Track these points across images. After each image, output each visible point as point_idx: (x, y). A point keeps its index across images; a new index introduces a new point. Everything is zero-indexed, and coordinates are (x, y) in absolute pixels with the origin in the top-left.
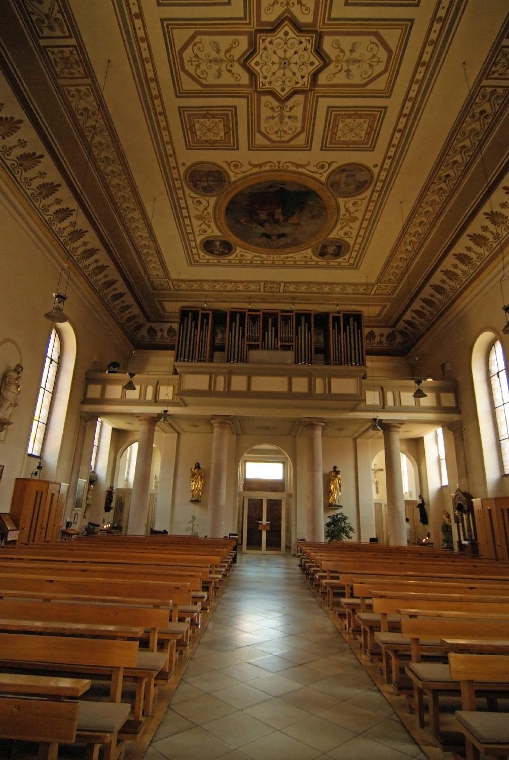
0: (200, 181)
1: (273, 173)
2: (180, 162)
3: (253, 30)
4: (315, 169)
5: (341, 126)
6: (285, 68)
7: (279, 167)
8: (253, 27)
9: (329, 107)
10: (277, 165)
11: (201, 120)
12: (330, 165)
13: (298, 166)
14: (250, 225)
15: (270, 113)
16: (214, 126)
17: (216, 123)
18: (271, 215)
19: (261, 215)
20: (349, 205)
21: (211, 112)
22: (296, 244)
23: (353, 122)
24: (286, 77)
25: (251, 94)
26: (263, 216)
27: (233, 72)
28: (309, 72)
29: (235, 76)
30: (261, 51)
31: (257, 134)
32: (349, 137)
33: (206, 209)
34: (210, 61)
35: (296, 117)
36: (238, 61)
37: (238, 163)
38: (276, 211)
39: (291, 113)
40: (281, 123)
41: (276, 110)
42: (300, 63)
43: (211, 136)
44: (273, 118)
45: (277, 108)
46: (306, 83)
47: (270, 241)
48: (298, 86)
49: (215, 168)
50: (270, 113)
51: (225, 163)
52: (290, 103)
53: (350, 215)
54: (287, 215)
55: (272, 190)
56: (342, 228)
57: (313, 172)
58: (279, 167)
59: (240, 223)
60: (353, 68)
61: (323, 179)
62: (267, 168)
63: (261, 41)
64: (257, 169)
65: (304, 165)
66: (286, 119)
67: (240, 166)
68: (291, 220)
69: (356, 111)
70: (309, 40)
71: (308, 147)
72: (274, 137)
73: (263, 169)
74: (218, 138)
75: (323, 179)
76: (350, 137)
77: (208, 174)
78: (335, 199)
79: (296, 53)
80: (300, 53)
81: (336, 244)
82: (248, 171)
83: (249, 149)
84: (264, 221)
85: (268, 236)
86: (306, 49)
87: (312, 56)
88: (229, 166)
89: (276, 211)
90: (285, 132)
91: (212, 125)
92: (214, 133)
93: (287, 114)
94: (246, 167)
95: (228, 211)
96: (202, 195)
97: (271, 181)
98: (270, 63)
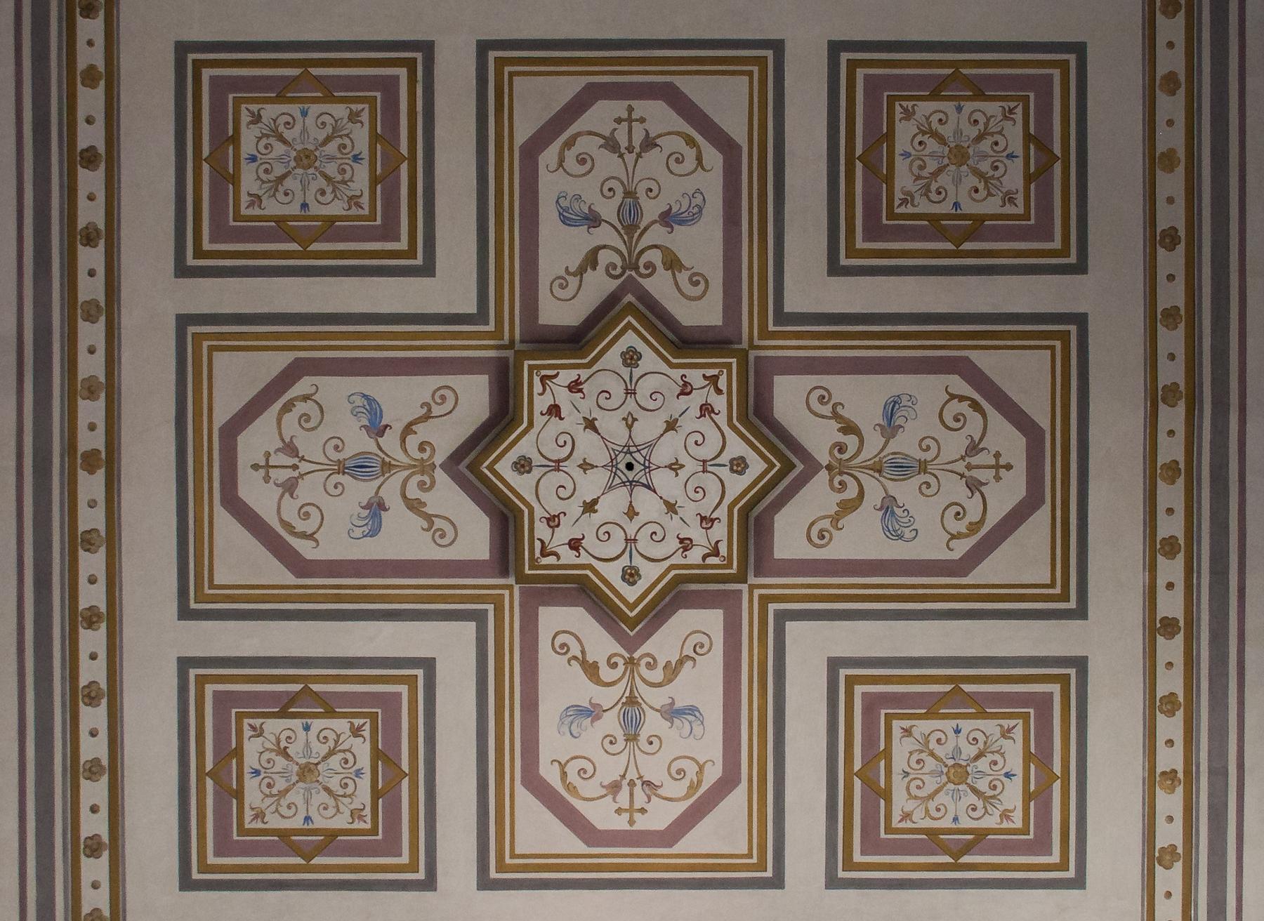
3: (752, 580)
5: (361, 179)
8: (752, 587)
9: (428, 269)
11: (992, 206)
16: (935, 175)
17: (926, 191)
24: (622, 413)
27: (835, 425)
29: (826, 410)
30: (722, 513)
32: (310, 121)
34: (923, 467)
35: (565, 221)
36: (812, 467)
39: (582, 240)
40: (629, 194)
41: (655, 256)
42: (571, 467)
43: (956, 118)
44: (667, 219)
45: (650, 266)
46: (538, 387)
48: (571, 375)
50: (681, 240)
52: (598, 286)
63: (723, 550)
66: (608, 210)
70: (544, 553)
72: (658, 115)
74: (925, 108)
79: (590, 507)
80: (574, 508)
83: (777, 46)
90: (611, 144)
91: (944, 180)
92: (942, 140)
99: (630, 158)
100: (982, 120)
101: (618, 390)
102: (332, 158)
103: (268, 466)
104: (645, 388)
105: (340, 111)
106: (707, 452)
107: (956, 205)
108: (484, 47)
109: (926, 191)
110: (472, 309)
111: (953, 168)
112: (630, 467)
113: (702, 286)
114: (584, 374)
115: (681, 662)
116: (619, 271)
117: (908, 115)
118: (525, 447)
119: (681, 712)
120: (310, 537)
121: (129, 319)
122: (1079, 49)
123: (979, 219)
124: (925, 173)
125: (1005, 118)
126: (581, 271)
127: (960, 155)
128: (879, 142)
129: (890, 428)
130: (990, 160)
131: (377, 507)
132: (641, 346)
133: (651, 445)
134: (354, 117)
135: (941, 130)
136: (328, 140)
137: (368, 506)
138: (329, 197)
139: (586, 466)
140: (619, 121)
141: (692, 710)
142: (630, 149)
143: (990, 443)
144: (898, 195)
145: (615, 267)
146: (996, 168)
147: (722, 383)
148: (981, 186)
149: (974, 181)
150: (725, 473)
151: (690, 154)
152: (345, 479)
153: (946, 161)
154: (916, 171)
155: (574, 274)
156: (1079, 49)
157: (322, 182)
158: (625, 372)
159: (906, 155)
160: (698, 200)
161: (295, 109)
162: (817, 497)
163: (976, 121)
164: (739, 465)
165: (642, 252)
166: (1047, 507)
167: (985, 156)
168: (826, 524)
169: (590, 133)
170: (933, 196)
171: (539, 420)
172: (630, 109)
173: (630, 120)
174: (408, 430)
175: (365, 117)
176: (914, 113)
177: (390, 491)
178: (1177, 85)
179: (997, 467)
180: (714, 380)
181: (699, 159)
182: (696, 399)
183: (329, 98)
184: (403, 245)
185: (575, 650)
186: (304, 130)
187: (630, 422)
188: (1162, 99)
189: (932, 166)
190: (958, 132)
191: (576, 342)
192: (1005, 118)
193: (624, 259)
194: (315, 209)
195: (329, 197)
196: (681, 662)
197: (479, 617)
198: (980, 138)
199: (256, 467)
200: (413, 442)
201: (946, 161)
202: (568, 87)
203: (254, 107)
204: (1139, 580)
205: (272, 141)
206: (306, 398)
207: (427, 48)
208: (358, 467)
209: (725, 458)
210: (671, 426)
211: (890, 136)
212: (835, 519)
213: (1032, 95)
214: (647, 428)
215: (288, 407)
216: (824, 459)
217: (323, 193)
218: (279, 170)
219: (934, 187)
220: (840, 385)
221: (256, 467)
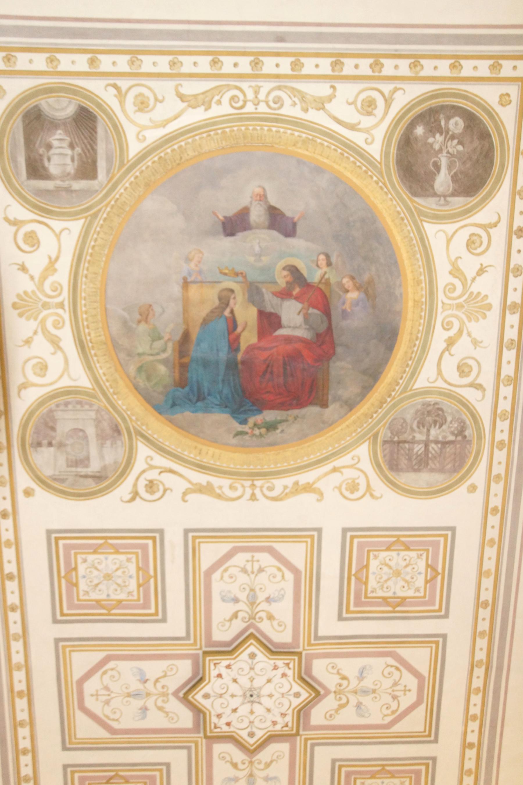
0: (445, 443)
1: (266, 469)
2: (479, 495)
4: (168, 479)
5: (133, 585)
6: (250, 690)
7: (253, 486)
9: (164, 620)
10: (257, 492)
11: (410, 593)
12: (135, 495)
13: (206, 490)
14: (333, 277)
15: (274, 608)
16: (386, 581)
17: (382, 588)
18: (269, 321)
19: (299, 320)
20: (55, 364)
21: (390, 609)
22: (183, 169)
25: (310, 644)
26: (294, 319)
28: (210, 684)
29: (335, 671)
30: (290, 712)
33: (451, 342)
35: (223, 600)
37: (347, 494)
39: (232, 608)
40: (252, 590)
41: (263, 615)
42: (227, 696)
43: (396, 558)
45: (261, 618)
47: (273, 201)
49: (406, 478)
50: (274, 608)
51: (377, 494)
52: (238, 626)
53: (43, 322)
55: (270, 415)
56: (52, 262)
57: (171, 471)
58: (253, 486)
60: (135, 686)
61: (143, 451)
62: (280, 484)
63: (290, 724)
64: (305, 478)
66: (243, 596)
69: (109, 614)
71: (194, 537)
72: (265, 559)
73: (289, 481)
74: (383, 555)
75: (143, 451)
76: (109, 562)
77: (421, 463)
78: (96, 381)
80: (228, 711)
81: (49, 185)
83: (319, 531)
84: (285, 294)
85: (280, 222)
86: (219, 716)
87: (209, 707)
88: (368, 486)
90: (244, 571)
91: (390, 583)
92: (390, 567)
93: (241, 606)
95: (387, 336)
96: (449, 395)
97: (272, 444)
98: (277, 695)
99: (253, 576)
101: (246, 668)
102: (120, 577)
103: (97, 695)
104: (258, 667)
105: (123, 557)
106: (285, 690)
107: (394, 593)
108: (186, 532)
110: (183, 634)
111: (394, 578)
112: (251, 696)
113: (282, 628)
114: (232, 662)
115: (272, 762)
116: (247, 620)
117: (376, 557)
118: (207, 689)
119: (271, 779)
120: (117, 720)
121: (33, 639)
122: (453, 529)
123: (404, 599)
124: (382, 580)
125: (418, 558)
126: (231, 620)
127: (397, 573)
128: (362, 568)
129: (361, 677)
130: (410, 575)
131: (144, 709)
132: (257, 652)
133: (261, 688)
134: (129, 560)
135: (391, 563)
136: (117, 569)
137: (141, 709)
138: (119, 592)
139: (233, 696)
140: (248, 561)
141: (275, 778)
142: (253, 572)
143: (403, 682)
144: (370, 589)
145: (245, 618)
146: (413, 578)
147: (291, 665)
148: (406, 585)
149: (402, 583)
150: (292, 698)
151: (279, 574)
152: (131, 699)
153: (391, 576)
154: (378, 579)
155: (228, 621)
156: (453, 529)
158: (250, 661)
160: (282, 592)
161: (102, 557)
162: (328, 703)
163: (405, 560)
164: (297, 695)
165: (257, 613)
166: (423, 706)
167: (407, 573)
168: (333, 712)
169: (235, 566)
170: (385, 589)
171: (213, 680)
172: (253, 557)
173: (253, 561)
174: (157, 681)
175: (134, 560)
176: (378, 556)
177: (150, 703)
178: (494, 543)
179: (405, 691)
180: (288, 664)
181: (283, 577)
182: (280, 672)
183: (117, 552)
184: (153, 611)
185: (228, 758)
187: (252, 680)
188: (487, 549)
189: (385, 577)
191: (229, 650)
192: (418, 558)
193: (249, 615)
194: (113, 597)
195: (119, 592)
196: (272, 762)
197: (189, 748)
198: (406, 566)
199: (92, 695)
200: (159, 685)
201: (391, 576)
202: (225, 548)
203: (84, 556)
204: (460, 729)
205: (93, 570)
206: (112, 669)
207: (161, 532)
208: (136, 695)
209: (292, 692)
210: (269, 681)
211: (367, 566)
212: (337, 711)
213: (431, 549)
214: (258, 682)
215: (105, 673)
216: (333, 688)
217: (116, 590)
218: (96, 581)
219: (385, 586)
220: (340, 662)
221: (92, 695)
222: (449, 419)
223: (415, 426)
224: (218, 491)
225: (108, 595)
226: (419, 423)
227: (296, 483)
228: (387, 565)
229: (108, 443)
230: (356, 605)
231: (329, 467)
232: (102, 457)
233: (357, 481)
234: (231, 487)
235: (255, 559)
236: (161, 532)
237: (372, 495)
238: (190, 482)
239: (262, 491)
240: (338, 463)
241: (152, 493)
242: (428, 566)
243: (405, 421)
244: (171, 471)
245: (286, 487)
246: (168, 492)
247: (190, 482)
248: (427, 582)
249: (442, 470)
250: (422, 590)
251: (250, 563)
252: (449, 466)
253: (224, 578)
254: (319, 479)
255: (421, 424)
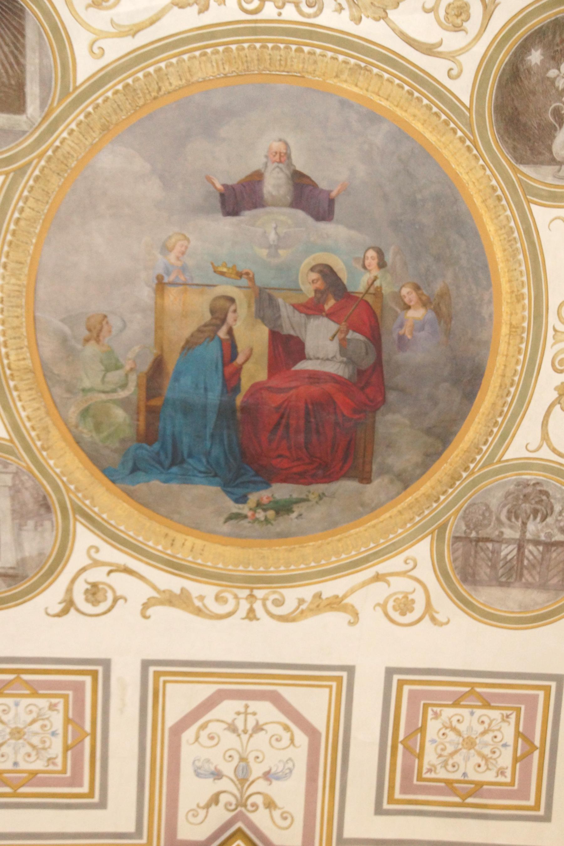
0: (549, 545)
1: (273, 572)
4: (121, 582)
5: (56, 747)
7: (251, 596)
9: (102, 805)
10: (258, 606)
11: (490, 776)
12: (69, 605)
13: (180, 600)
14: (387, 286)
15: (276, 790)
16: (452, 754)
18: (286, 349)
19: (333, 348)
21: (457, 799)
23: (20, 759)
26: (323, 345)
31: (321, 726)
32: (21, 708)
35: (198, 775)
37: (396, 616)
38: (262, 376)
39: (210, 787)
40: (242, 759)
41: (258, 800)
43: (469, 720)
44: (267, 776)
47: (300, 163)
49: (488, 596)
50: (276, 790)
51: (441, 617)
54: (216, 339)
55: (281, 491)
57: (127, 570)
59: (425, 303)
61: (84, 538)
62: (291, 596)
65: (161, 603)
66: (228, 769)
67: (391, 604)
68: (189, 311)
69: (15, 795)
71: (156, 674)
72: (265, 711)
73: (307, 592)
74: (448, 712)
75: (84, 538)
77: (512, 574)
82: (364, 584)
83: (351, 670)
84: (312, 308)
85: (308, 197)
88: (428, 604)
89: (262, 376)
90: (232, 728)
91: (458, 758)
92: (459, 733)
93: (224, 784)
94: (367, 599)
95: (467, 379)
97: (282, 535)
99: (245, 737)
100: (487, 721)
102: (36, 734)
105: (43, 703)
107: (465, 774)
108: (146, 664)
109: (445, 764)
110: (131, 828)
111: (464, 751)
113: (289, 821)
116: (233, 807)
117: (437, 716)
123: (479, 785)
124: (445, 753)
125: (503, 720)
126: (207, 806)
127: (470, 743)
130: (491, 747)
134: (52, 707)
136: (34, 721)
138: (33, 758)
140: (238, 713)
144: (426, 766)
145: (231, 804)
146: (494, 752)
148: (483, 763)
149: (478, 760)
151: (286, 736)
153: (460, 746)
154: (439, 751)
155: (203, 808)
157: (28, 749)
159: (433, 741)
160: (290, 765)
163: (483, 722)
165: (250, 796)
167: (486, 744)
169: (218, 721)
170: (450, 768)
172: (247, 707)
173: (246, 713)
175: (61, 707)
176: (441, 715)
181: (292, 740)
183: (35, 694)
186: (16, 715)
189: (450, 749)
190: (470, 728)
192: (503, 720)
193: (237, 800)
194: (23, 766)
195: (33, 758)
198: (484, 733)
201: (460, 746)
207: (106, 664)
211: (423, 730)
213: (523, 707)
217: (29, 755)
219: (450, 762)
222: (557, 508)
223: (503, 518)
224: (198, 603)
225: (16, 764)
226: (509, 512)
227: (318, 596)
228: (454, 729)
229: (31, 524)
230: (404, 791)
231: (368, 573)
232: (19, 544)
233: (410, 597)
234: (218, 598)
235: (250, 710)
236: (106, 664)
237: (433, 620)
238: (154, 587)
239: (264, 605)
240: (383, 567)
241: (96, 603)
242: (518, 734)
243: (488, 508)
244: (127, 570)
245: (301, 601)
246: (121, 602)
247: (154, 587)
248: (516, 760)
249: (543, 586)
250: (509, 773)
251: (242, 717)
252: (555, 581)
253: (200, 740)
254: (353, 591)
255: (513, 514)
